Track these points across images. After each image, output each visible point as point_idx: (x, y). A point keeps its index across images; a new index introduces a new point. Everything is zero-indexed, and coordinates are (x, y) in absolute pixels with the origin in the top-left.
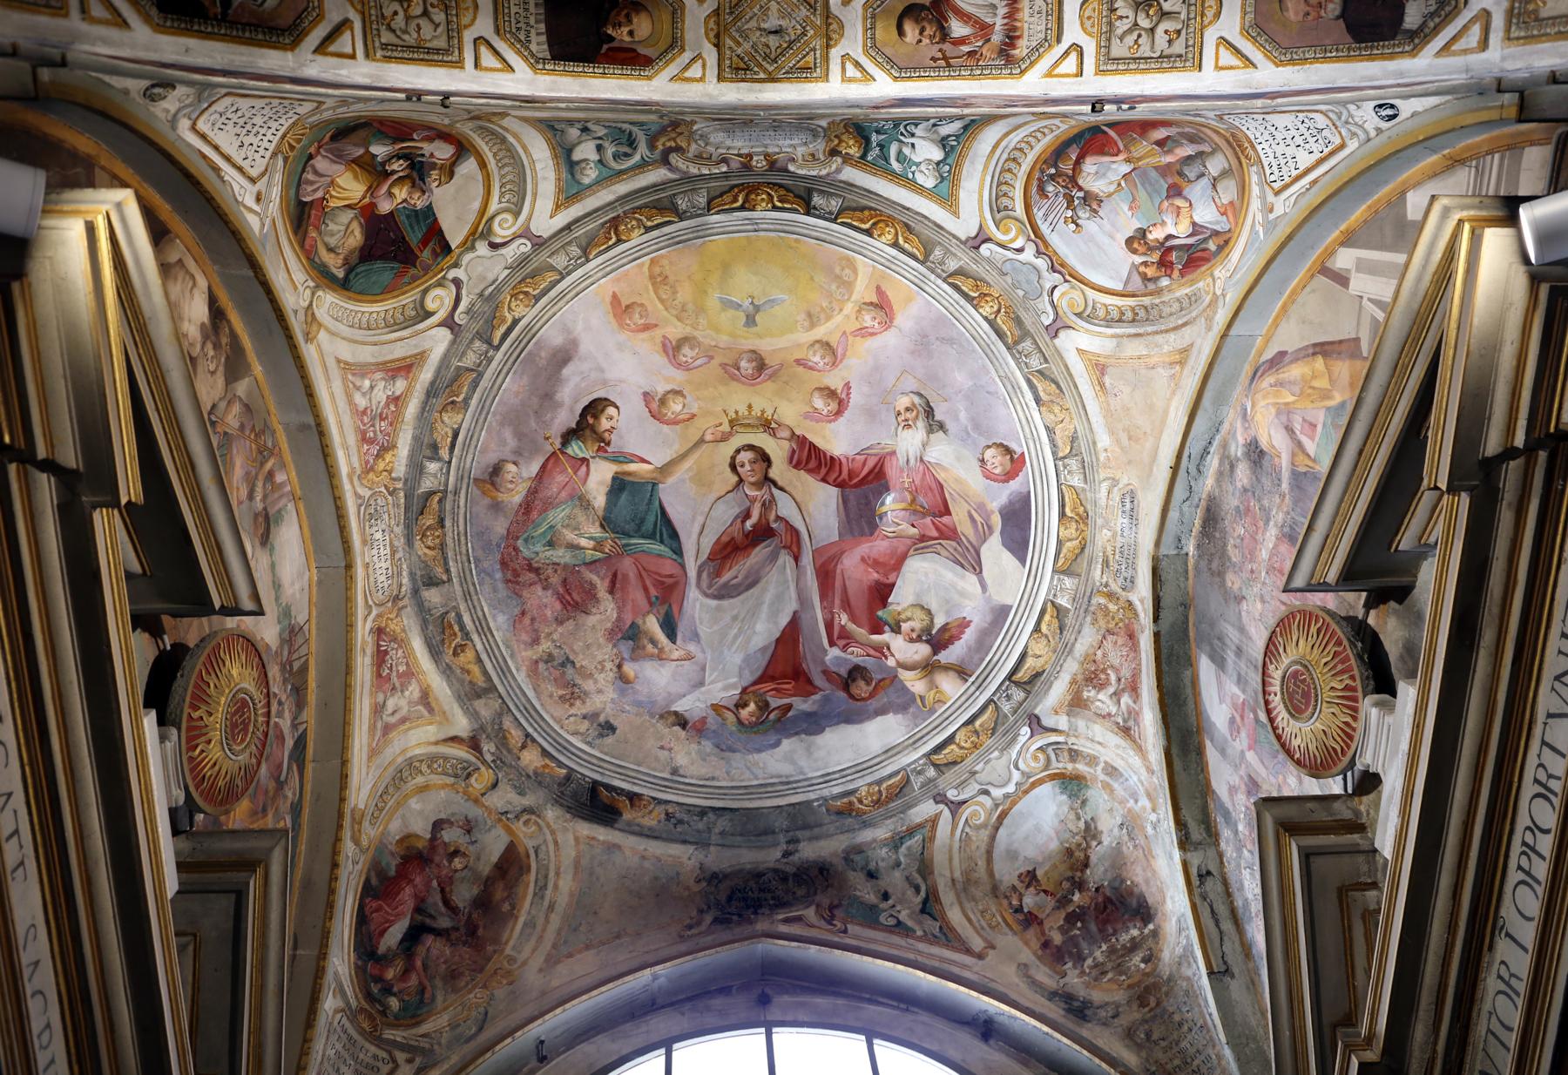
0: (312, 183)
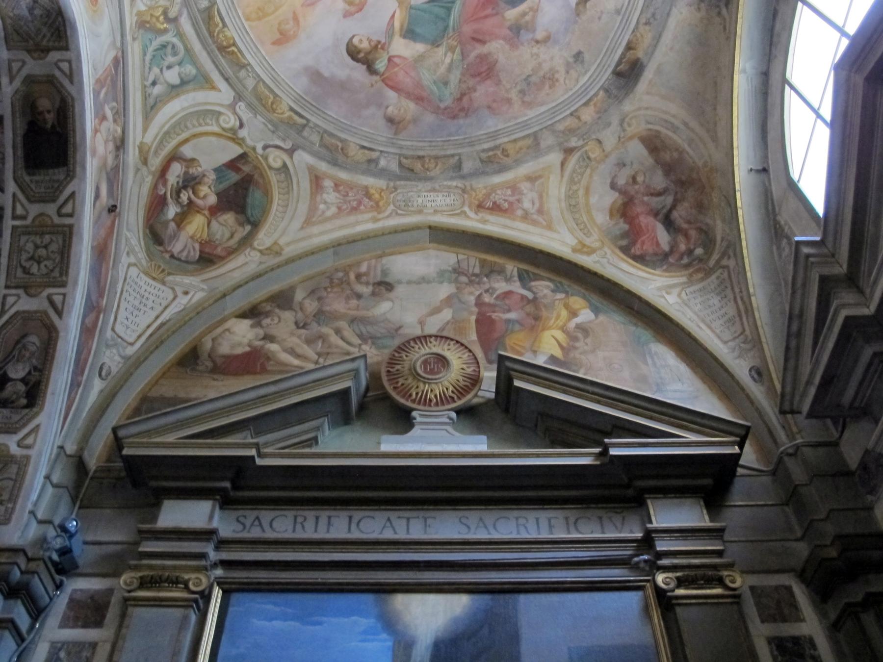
0: (189, 252)
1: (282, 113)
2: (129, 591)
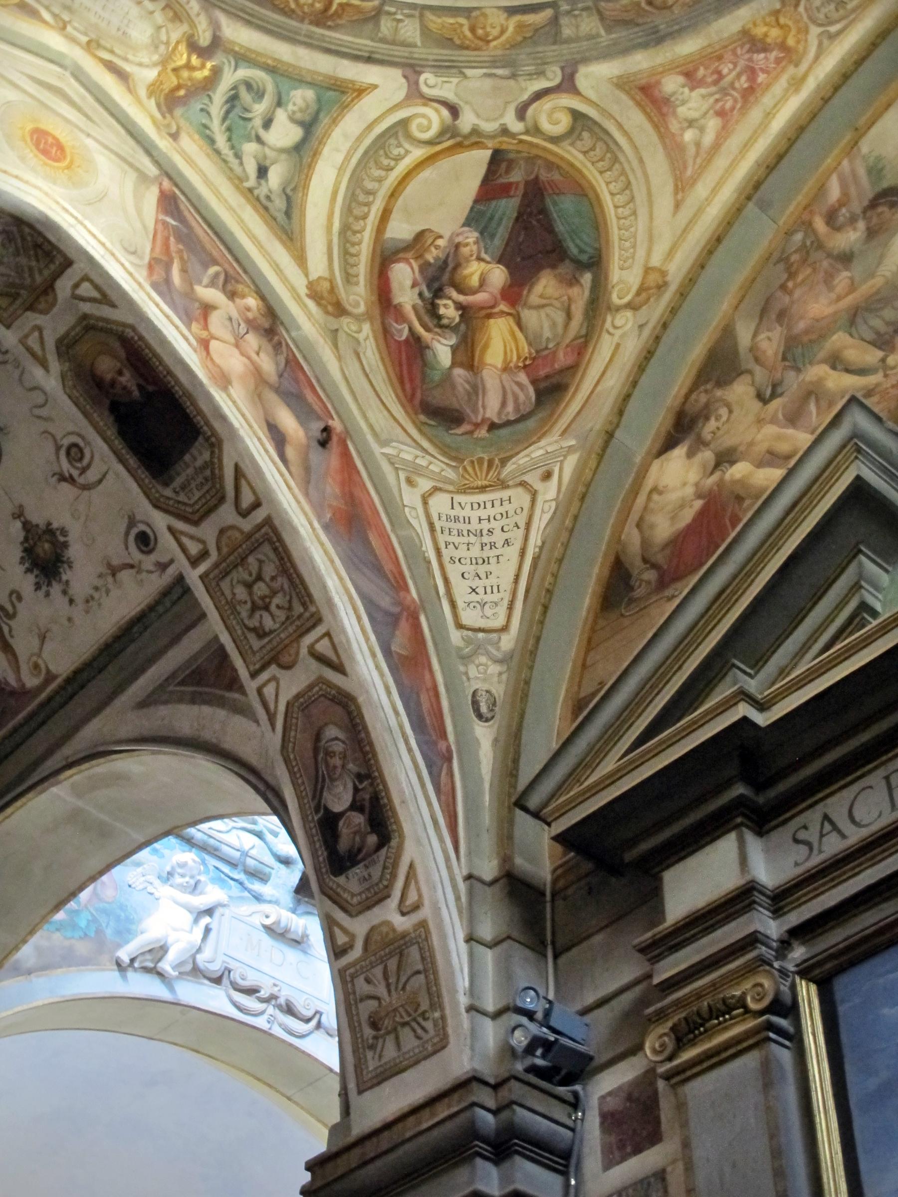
1: (503, 32)
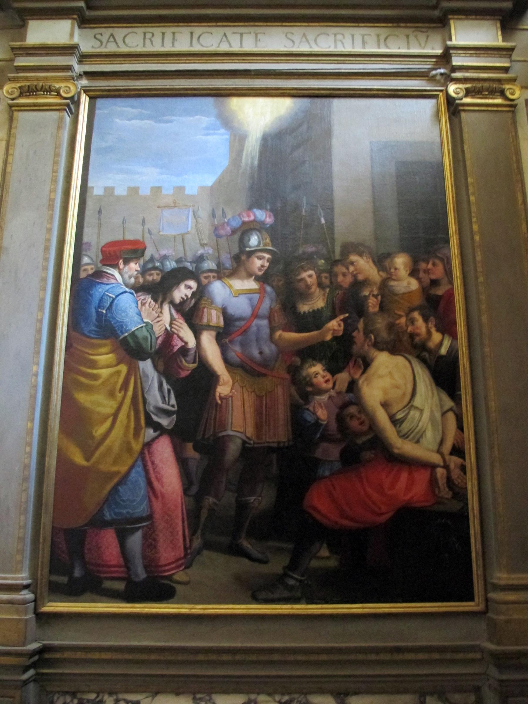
2: (13, 99)
